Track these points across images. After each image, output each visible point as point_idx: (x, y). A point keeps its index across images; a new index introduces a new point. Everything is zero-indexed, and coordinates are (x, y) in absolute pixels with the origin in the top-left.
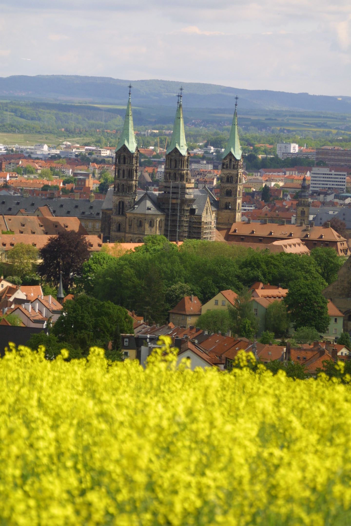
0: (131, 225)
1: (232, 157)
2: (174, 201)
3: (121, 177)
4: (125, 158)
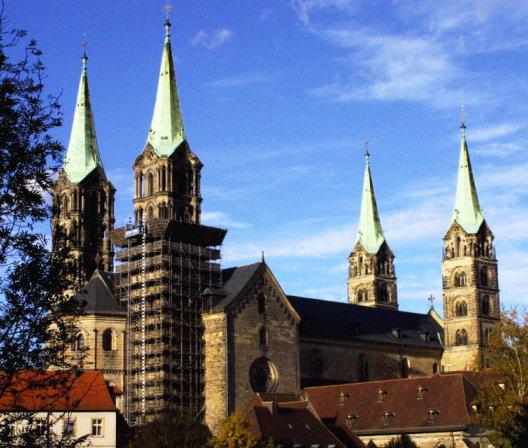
1: (460, 231)
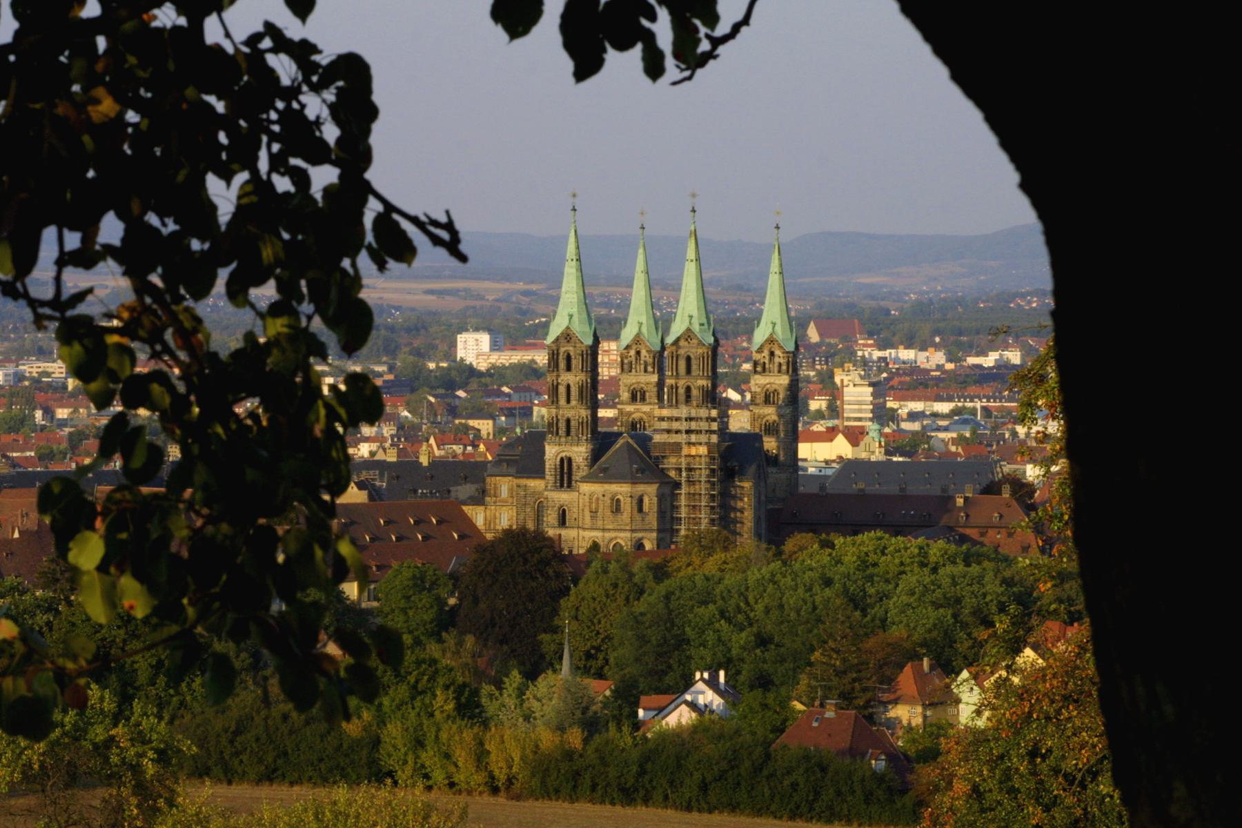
0: (596, 512)
1: (776, 345)
2: (693, 451)
3: (562, 401)
4: (569, 358)
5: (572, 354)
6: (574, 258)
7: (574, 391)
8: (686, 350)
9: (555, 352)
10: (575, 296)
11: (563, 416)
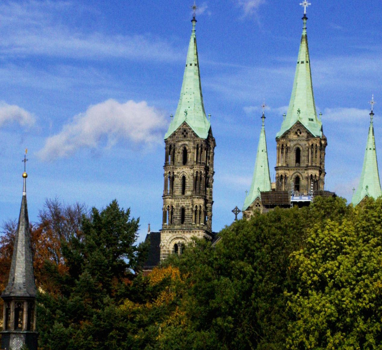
4: (185, 153)
5: (187, 148)
6: (194, 62)
7: (190, 182)
8: (295, 143)
9: (173, 146)
10: (192, 96)
11: (178, 206)
